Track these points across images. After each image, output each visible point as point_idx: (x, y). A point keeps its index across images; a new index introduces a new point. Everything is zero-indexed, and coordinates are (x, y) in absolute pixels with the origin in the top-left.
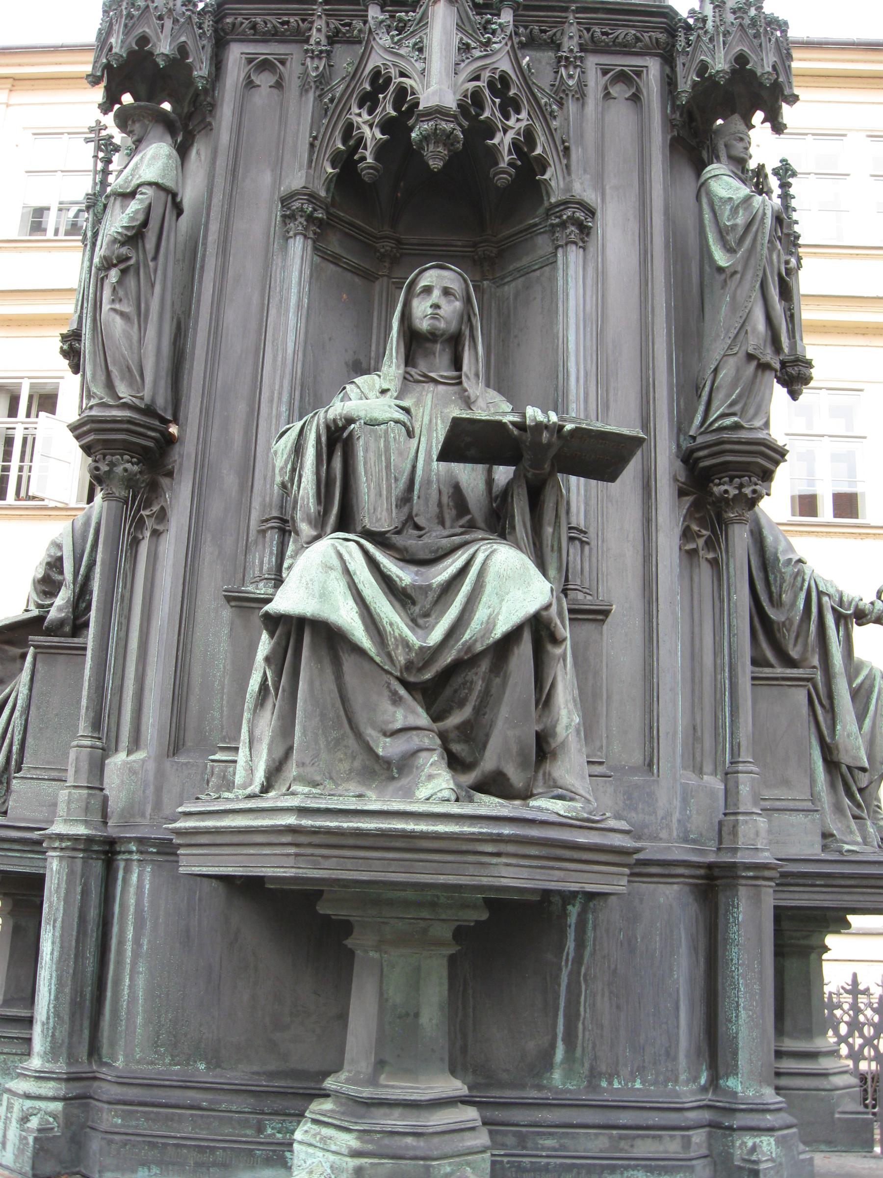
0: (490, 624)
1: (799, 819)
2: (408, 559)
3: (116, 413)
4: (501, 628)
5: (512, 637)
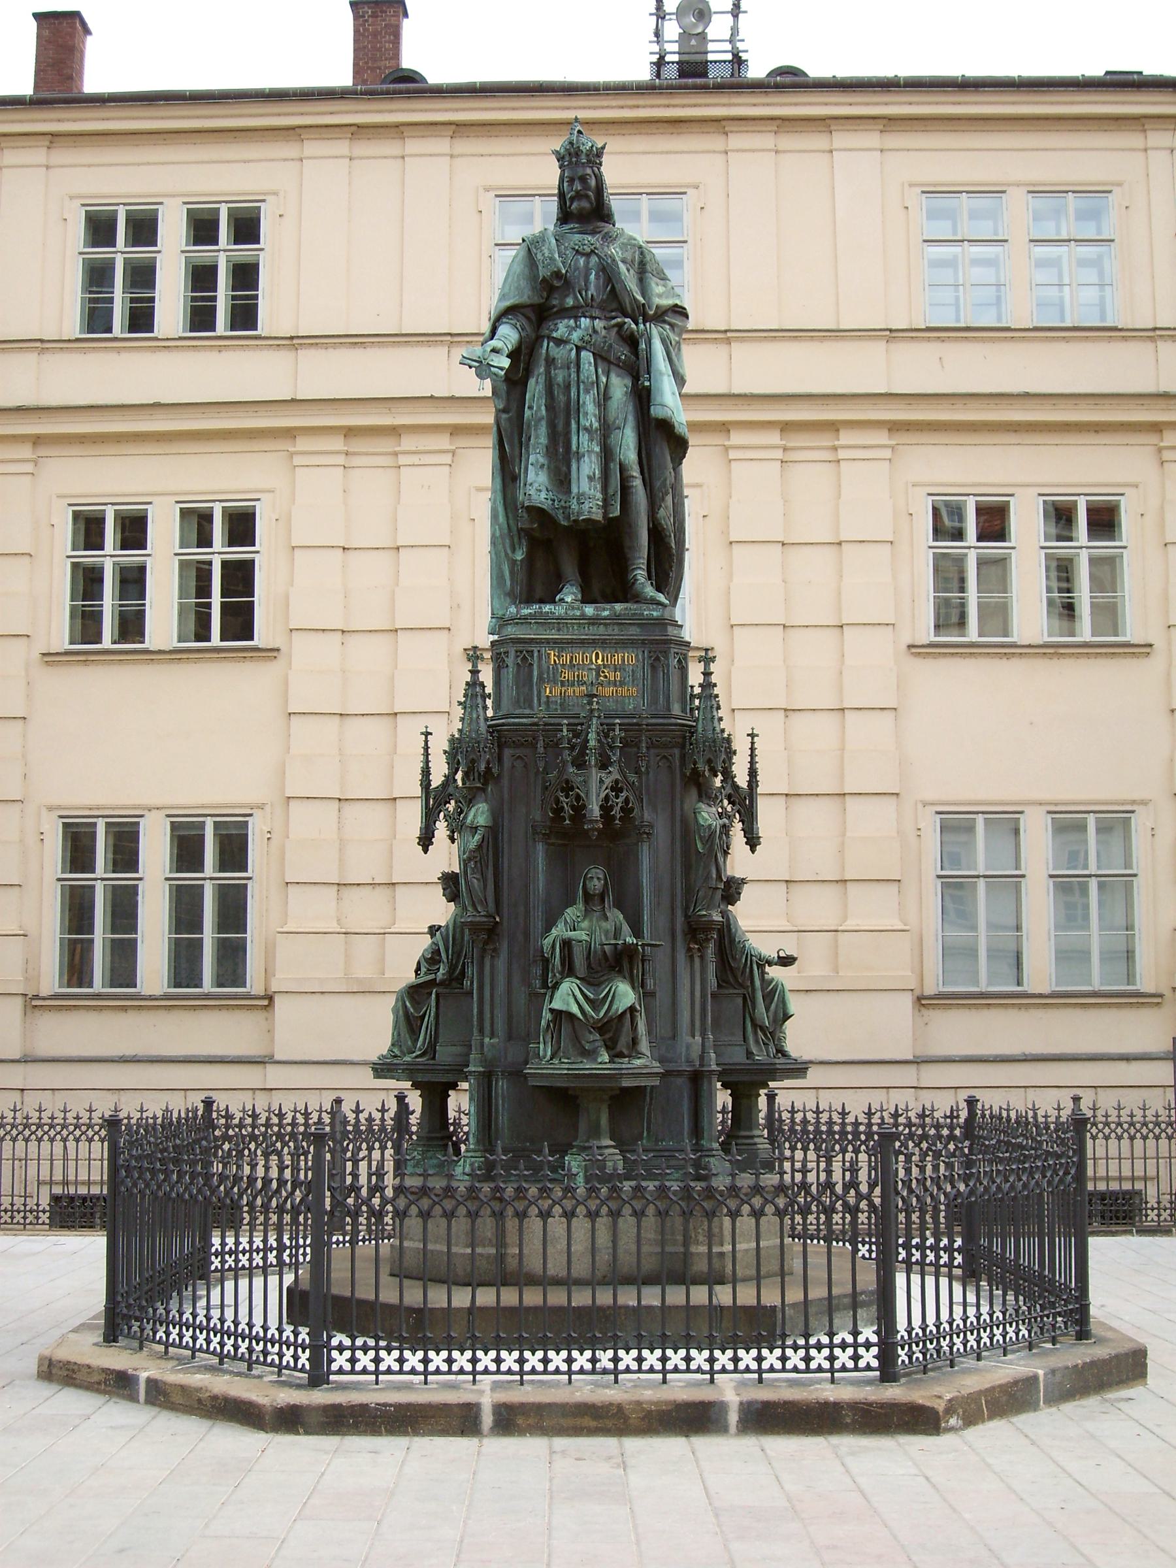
0: (617, 1009)
1: (737, 1048)
3: (478, 919)
4: (620, 1011)
5: (624, 1013)
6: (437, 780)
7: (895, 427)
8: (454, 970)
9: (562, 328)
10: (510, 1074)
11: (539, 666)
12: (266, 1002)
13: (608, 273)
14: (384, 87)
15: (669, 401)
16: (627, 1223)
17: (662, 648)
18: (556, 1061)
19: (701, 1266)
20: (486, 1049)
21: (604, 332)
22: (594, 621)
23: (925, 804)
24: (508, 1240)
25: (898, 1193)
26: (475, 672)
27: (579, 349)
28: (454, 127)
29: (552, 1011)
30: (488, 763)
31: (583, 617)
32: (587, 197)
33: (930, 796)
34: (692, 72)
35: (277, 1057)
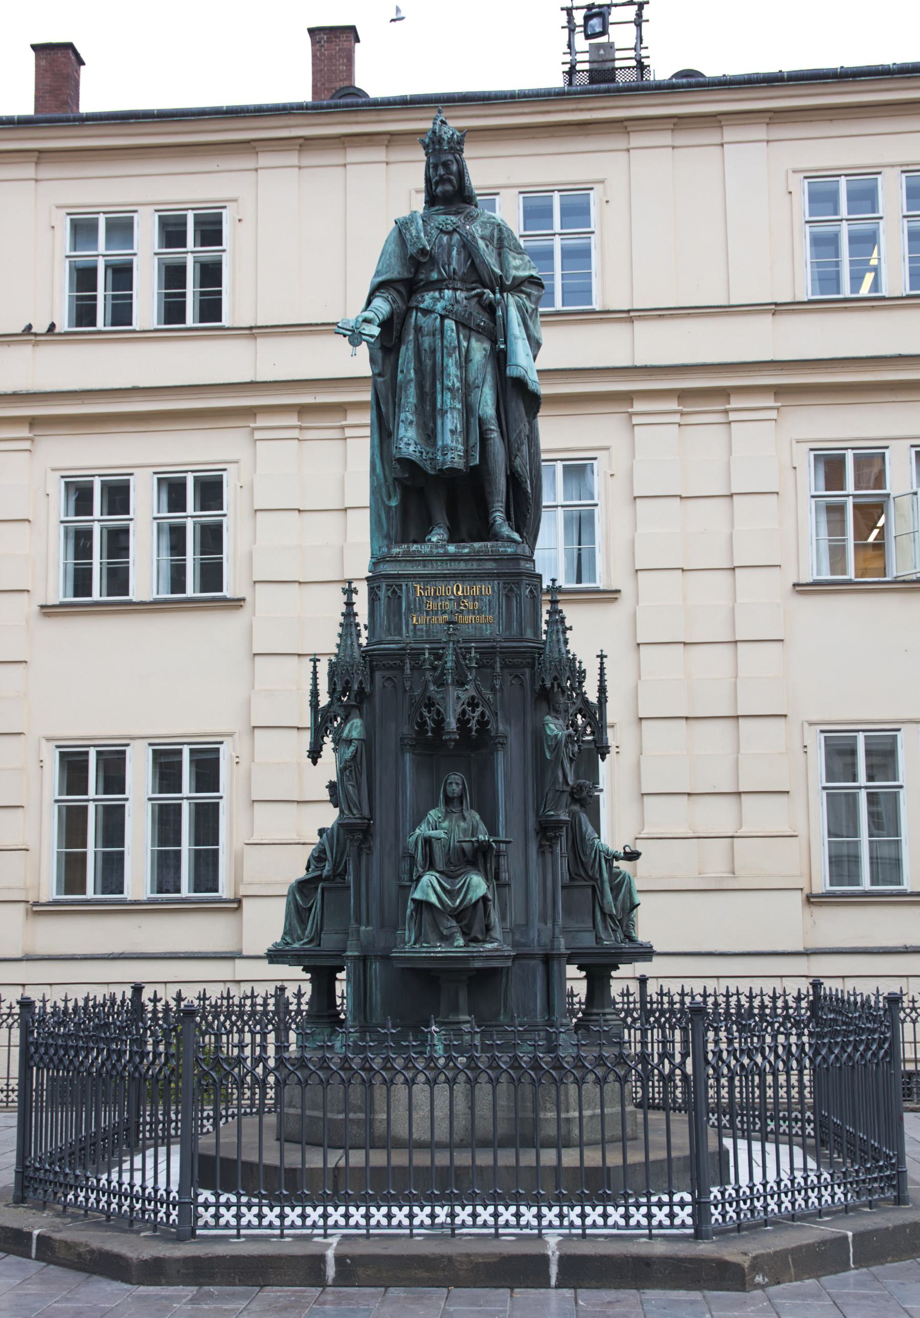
0: (471, 899)
2: (448, 876)
4: (474, 900)
5: (477, 901)
7: (779, 391)
8: (339, 867)
9: (428, 299)
10: (381, 956)
11: (408, 597)
12: (235, 905)
13: (468, 248)
14: (332, 102)
15: (524, 362)
16: (484, 1090)
17: (517, 579)
18: (417, 946)
19: (550, 1131)
20: (362, 935)
21: (465, 302)
22: (455, 558)
23: (811, 724)
24: (377, 1107)
25: (708, 1063)
26: (349, 604)
27: (443, 317)
28: (388, 137)
29: (414, 900)
30: (361, 683)
31: (446, 554)
32: (450, 181)
33: (815, 718)
34: (601, 79)
35: (245, 953)
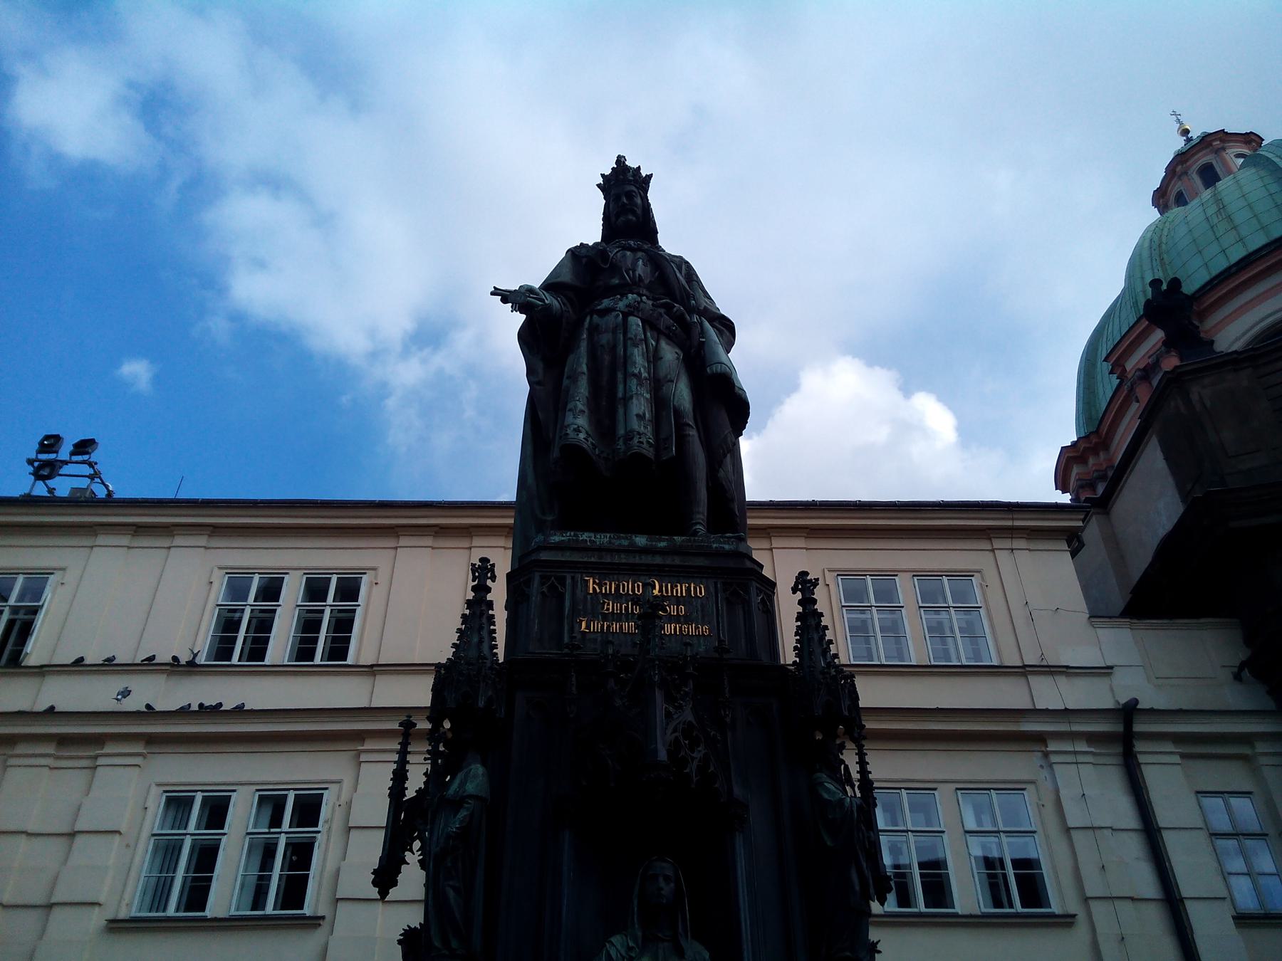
6: (415, 781)
9: (606, 303)
26: (481, 589)
32: (634, 213)
